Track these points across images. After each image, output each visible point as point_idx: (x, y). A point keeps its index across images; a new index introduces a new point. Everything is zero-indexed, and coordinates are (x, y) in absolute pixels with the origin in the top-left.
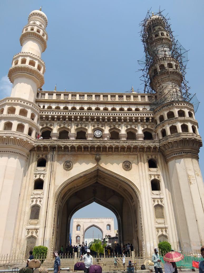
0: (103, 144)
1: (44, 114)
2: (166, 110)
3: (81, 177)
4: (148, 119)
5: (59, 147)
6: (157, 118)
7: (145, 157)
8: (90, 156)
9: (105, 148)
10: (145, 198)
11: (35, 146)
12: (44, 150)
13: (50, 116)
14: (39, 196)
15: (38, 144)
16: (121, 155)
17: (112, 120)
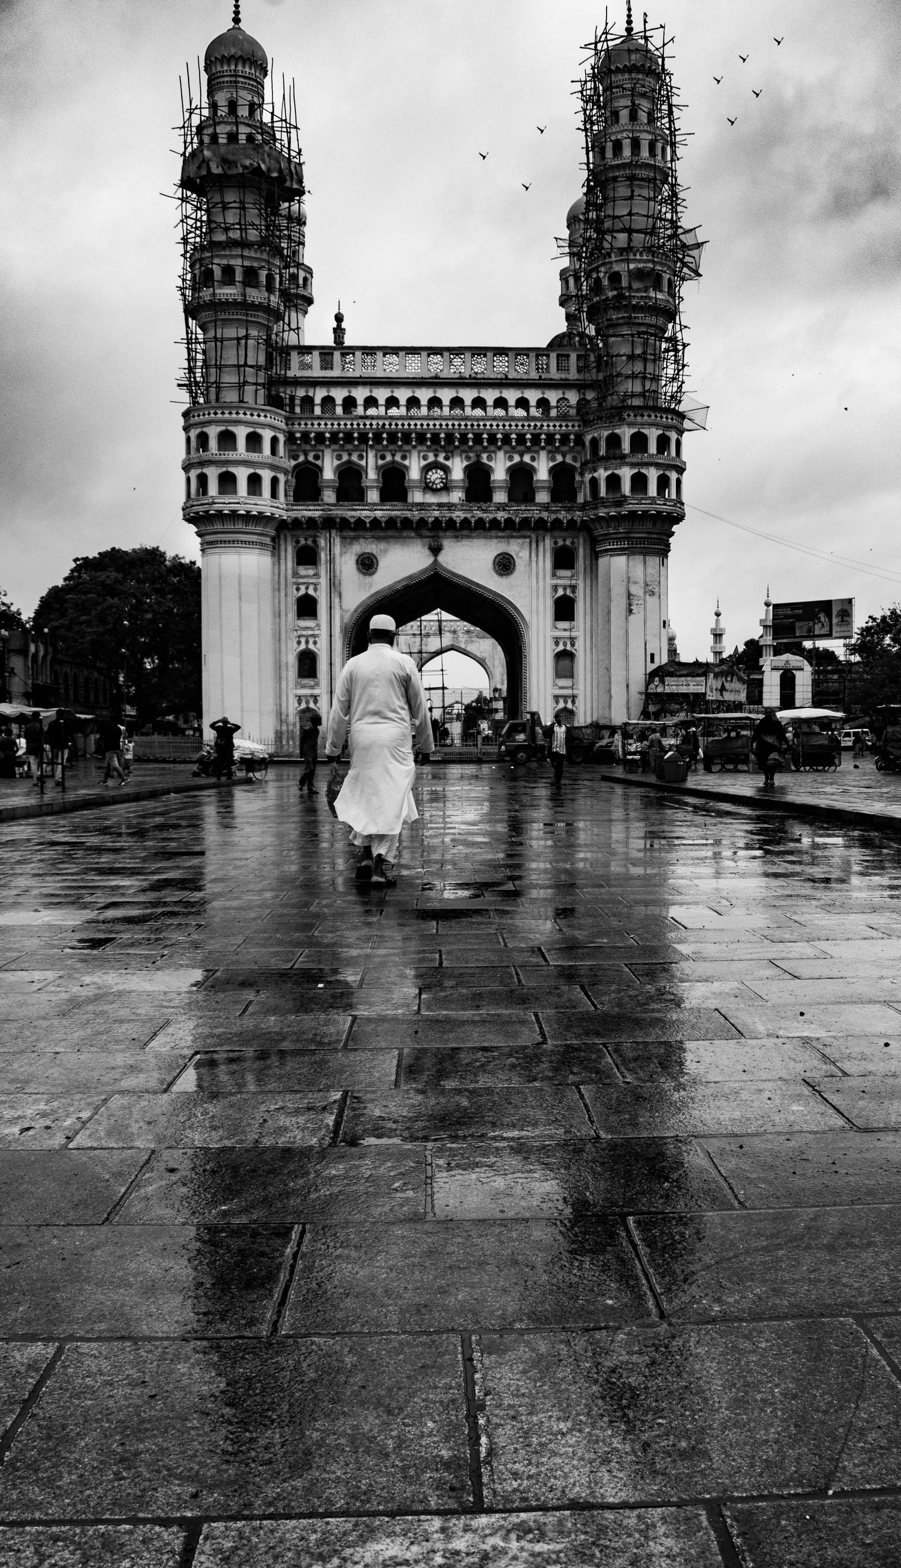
0: (448, 515)
1: (299, 429)
2: (606, 428)
3: (398, 591)
4: (565, 438)
5: (344, 520)
6: (588, 438)
7: (548, 542)
8: (419, 541)
9: (451, 521)
10: (538, 638)
11: (289, 521)
12: (308, 529)
13: (312, 435)
14: (310, 632)
15: (294, 514)
16: (491, 537)
17: (471, 443)
